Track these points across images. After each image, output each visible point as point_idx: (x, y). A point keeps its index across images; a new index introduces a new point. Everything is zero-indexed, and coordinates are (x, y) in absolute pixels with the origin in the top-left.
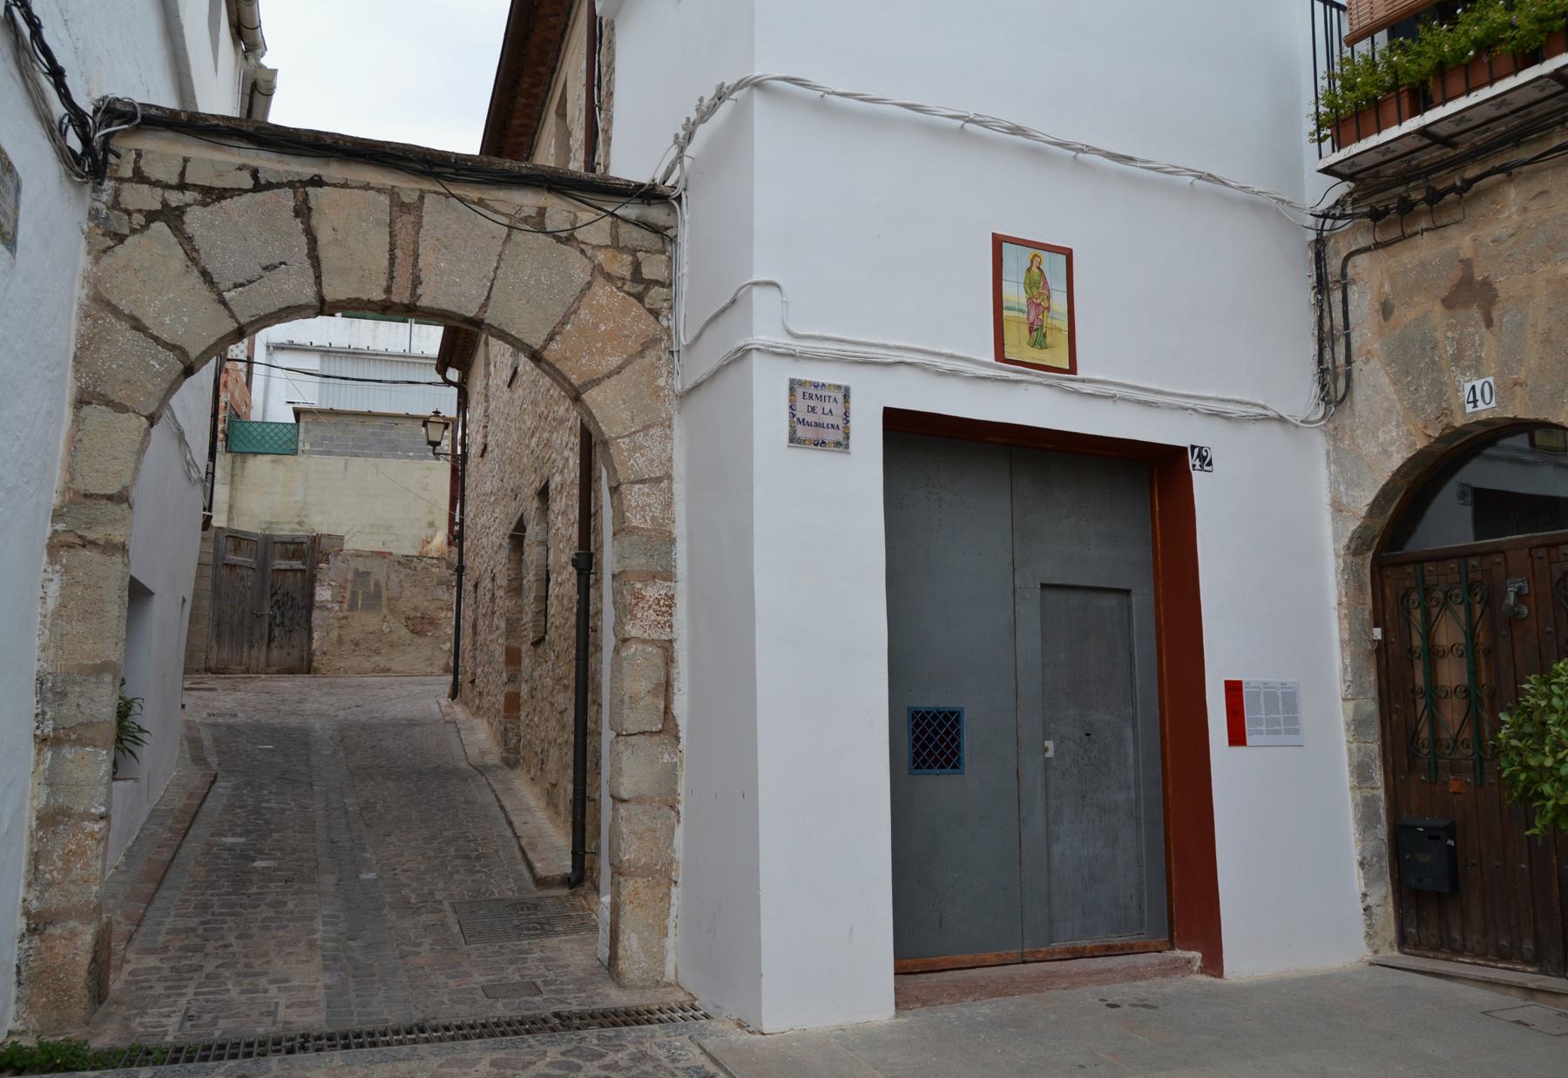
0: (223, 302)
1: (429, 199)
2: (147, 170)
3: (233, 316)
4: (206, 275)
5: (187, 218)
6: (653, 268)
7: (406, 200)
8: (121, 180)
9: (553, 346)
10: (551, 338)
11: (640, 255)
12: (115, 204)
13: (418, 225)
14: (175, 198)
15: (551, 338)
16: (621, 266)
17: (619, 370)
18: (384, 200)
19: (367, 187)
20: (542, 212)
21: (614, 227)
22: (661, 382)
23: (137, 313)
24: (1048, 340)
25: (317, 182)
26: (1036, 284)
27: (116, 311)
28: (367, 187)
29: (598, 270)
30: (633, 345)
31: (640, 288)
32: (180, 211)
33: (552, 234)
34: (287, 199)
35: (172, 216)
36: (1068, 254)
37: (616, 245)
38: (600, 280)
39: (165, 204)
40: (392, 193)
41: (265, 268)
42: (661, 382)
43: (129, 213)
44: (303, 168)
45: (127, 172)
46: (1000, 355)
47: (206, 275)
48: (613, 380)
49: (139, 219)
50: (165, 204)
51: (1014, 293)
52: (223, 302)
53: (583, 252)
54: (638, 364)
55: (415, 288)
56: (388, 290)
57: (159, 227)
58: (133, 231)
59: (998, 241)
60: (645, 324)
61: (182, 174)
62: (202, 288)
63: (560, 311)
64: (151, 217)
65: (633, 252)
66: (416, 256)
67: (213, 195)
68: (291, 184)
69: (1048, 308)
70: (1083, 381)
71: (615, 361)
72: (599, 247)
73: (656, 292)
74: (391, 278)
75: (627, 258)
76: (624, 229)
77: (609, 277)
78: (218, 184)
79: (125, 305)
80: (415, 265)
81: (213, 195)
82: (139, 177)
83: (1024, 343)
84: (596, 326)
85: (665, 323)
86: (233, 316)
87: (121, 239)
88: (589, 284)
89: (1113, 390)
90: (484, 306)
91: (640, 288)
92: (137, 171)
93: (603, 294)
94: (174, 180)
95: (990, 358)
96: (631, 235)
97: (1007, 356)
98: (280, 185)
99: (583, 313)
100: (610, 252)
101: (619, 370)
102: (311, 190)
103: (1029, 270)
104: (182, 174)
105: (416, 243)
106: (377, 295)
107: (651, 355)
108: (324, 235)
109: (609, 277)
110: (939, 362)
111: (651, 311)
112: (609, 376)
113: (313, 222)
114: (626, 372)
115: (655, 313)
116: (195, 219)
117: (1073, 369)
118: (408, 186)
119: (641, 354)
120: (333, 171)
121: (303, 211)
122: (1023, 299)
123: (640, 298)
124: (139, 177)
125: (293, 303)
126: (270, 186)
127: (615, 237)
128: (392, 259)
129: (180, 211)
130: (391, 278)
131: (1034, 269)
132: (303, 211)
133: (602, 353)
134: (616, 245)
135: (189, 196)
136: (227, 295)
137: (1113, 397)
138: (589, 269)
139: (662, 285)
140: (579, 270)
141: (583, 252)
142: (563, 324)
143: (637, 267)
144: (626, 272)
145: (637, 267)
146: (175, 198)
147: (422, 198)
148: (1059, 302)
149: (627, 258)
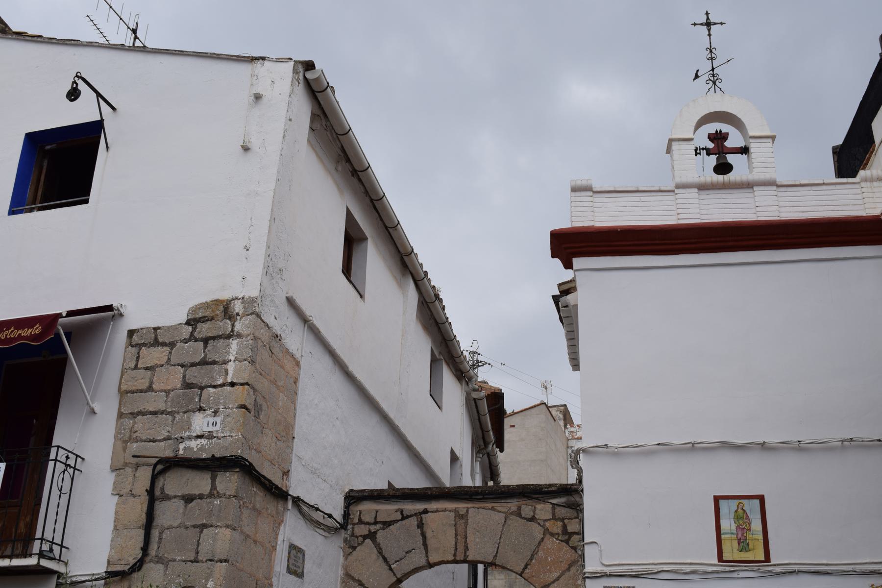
0: (391, 569)
1: (471, 511)
2: (363, 518)
3: (395, 575)
4: (385, 559)
5: (377, 536)
6: (572, 527)
7: (461, 513)
8: (354, 524)
9: (527, 571)
10: (526, 567)
11: (566, 521)
12: (353, 535)
13: (466, 524)
14: (373, 528)
15: (526, 567)
16: (557, 528)
17: (558, 579)
18: (453, 514)
19: (445, 510)
20: (519, 508)
21: (553, 509)
22: (579, 582)
23: (361, 579)
24: (751, 546)
25: (426, 511)
26: (741, 518)
27: (353, 579)
28: (445, 510)
29: (546, 531)
30: (564, 566)
31: (567, 537)
32: (375, 532)
33: (524, 518)
34: (414, 521)
35: (372, 536)
36: (761, 499)
37: (554, 518)
38: (548, 536)
39: (370, 531)
40: (456, 511)
41: (407, 553)
42: (579, 582)
43: (357, 537)
44: (420, 506)
45: (356, 521)
46: (720, 558)
47: (385, 559)
48: (556, 584)
49: (361, 539)
50: (370, 531)
51: (728, 525)
52: (391, 569)
53: (539, 524)
54: (567, 574)
55: (465, 553)
56: (455, 555)
57: (368, 541)
58: (359, 545)
59: (717, 499)
60: (570, 555)
61: (376, 518)
62: (383, 564)
63: (529, 553)
64: (365, 537)
65: (562, 520)
66: (466, 538)
67: (387, 524)
68: (416, 514)
69: (750, 530)
70: (775, 565)
71: (556, 575)
72: (546, 520)
73: (575, 538)
74: (456, 549)
75: (560, 524)
76: (558, 509)
77: (552, 535)
78: (388, 520)
79: (356, 576)
80: (466, 542)
81: (387, 524)
82: (361, 522)
83: (735, 551)
84: (546, 558)
85: (580, 553)
86: (395, 575)
87: (354, 548)
88: (543, 539)
89: (796, 568)
90: (496, 556)
91: (567, 537)
92: (360, 519)
93: (551, 543)
94: (372, 521)
95: (716, 561)
96: (562, 512)
97: (725, 558)
98: (411, 516)
99: (540, 553)
100: (552, 522)
101: (558, 579)
102: (423, 516)
103: (736, 511)
104: (376, 518)
105: (466, 532)
106: (451, 558)
107: (573, 569)
108: (429, 534)
109: (552, 535)
110: (684, 567)
111: (572, 548)
112: (553, 582)
113: (425, 529)
114: (561, 580)
115: (574, 548)
116: (380, 536)
117: (768, 558)
118: (461, 506)
119: (568, 569)
120: (433, 506)
121: (421, 525)
122: (734, 527)
123: (567, 542)
124: (361, 522)
125: (417, 566)
126: (408, 517)
127: (554, 514)
128: (456, 539)
129: (375, 532)
130: (456, 549)
131: (740, 510)
132: (421, 525)
133: (550, 571)
134: (554, 518)
135: (378, 526)
136: (393, 566)
137: (795, 572)
138: (542, 532)
139: (578, 534)
140: (537, 531)
141: (539, 524)
142: (531, 559)
143: (565, 527)
144: (559, 530)
145: (565, 527)
146: (373, 528)
147: (467, 511)
148: (757, 525)
149: (560, 524)
